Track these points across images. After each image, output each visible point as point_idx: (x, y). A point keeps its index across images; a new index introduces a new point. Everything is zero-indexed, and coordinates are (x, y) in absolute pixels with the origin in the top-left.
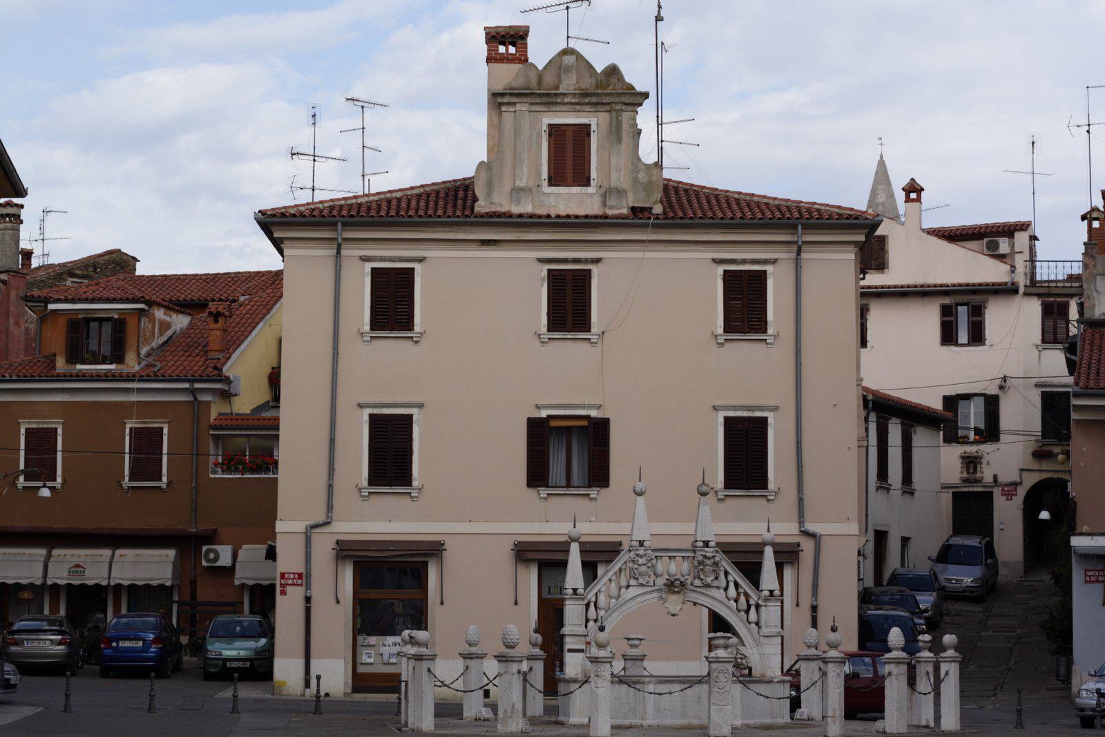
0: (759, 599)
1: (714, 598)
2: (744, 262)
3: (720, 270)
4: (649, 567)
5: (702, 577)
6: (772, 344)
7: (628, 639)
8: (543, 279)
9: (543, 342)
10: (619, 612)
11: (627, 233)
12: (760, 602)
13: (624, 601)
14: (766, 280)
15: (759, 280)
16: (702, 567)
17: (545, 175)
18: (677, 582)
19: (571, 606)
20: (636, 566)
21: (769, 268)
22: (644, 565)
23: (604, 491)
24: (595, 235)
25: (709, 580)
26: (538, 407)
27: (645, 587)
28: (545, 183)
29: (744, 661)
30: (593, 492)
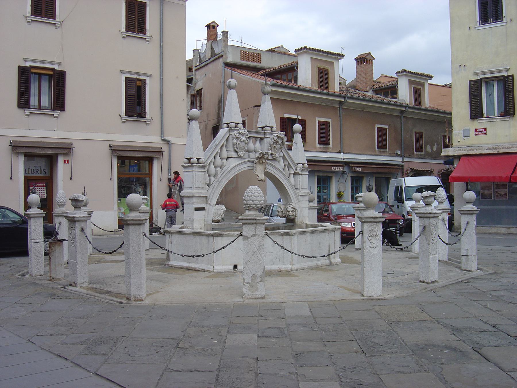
0: (296, 170)
4: (246, 143)
6: (148, 41)
9: (28, 22)
19: (196, 173)
20: (239, 142)
23: (62, 113)
26: (25, 60)
29: (294, 213)
30: (56, 113)
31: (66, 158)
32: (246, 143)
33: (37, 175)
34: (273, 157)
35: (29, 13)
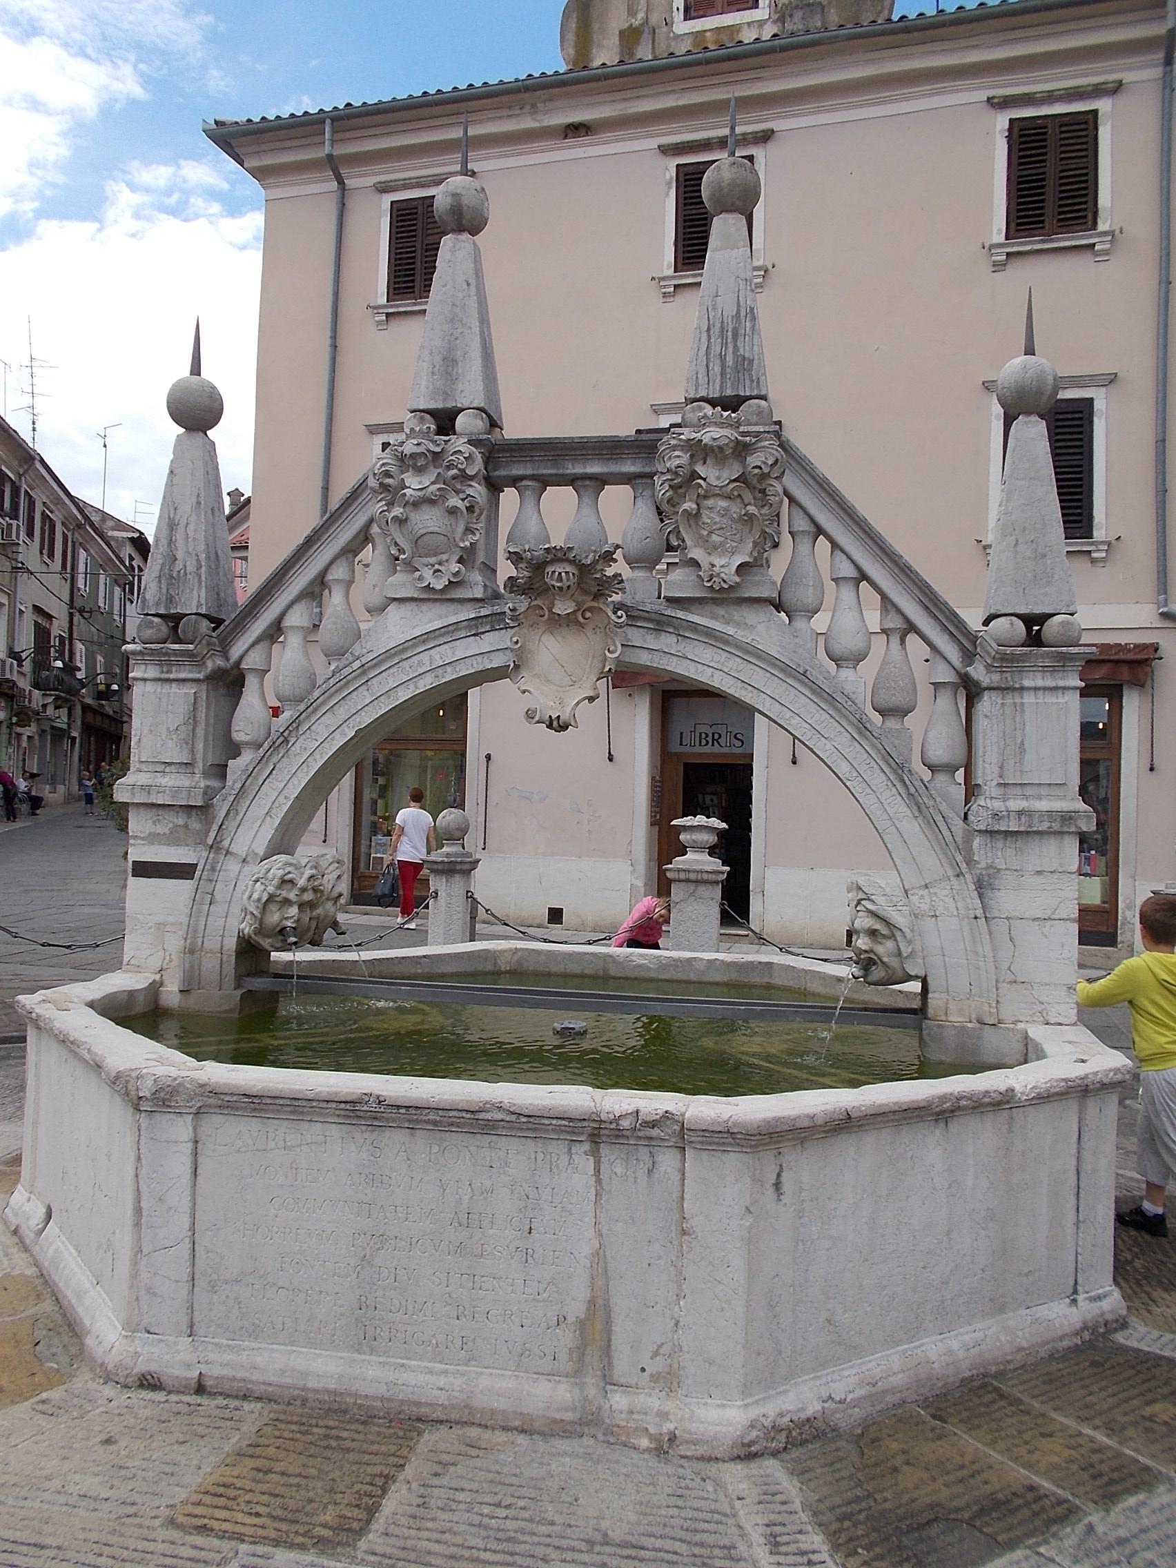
0: (969, 657)
1: (752, 653)
3: (1002, 121)
4: (453, 511)
8: (669, 183)
10: (342, 712)
11: (819, 70)
12: (978, 672)
13: (357, 664)
14: (1096, 129)
15: (1082, 130)
16: (689, 505)
18: (559, 568)
19: (150, 687)
20: (397, 511)
21: (1103, 105)
22: (431, 502)
24: (760, 84)
25: (726, 565)
26: (657, 410)
27: (452, 607)
28: (679, 16)
35: (669, 267)
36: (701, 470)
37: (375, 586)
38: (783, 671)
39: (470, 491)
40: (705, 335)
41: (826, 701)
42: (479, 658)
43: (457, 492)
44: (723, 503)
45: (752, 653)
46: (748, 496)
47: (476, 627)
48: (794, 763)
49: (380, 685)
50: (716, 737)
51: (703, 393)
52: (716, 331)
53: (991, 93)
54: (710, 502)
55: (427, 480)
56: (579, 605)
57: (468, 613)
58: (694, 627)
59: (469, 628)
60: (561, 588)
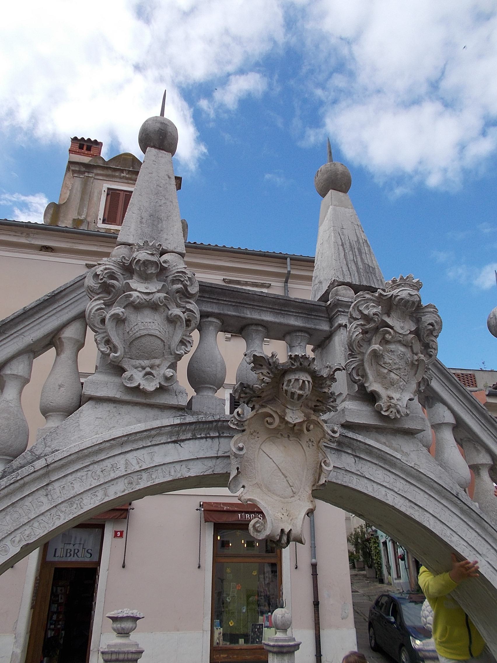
1: (414, 476)
2: (246, 284)
4: (172, 321)
5: (374, 386)
7: (115, 619)
13: (40, 464)
17: (101, 216)
18: (305, 377)
20: (117, 310)
22: (154, 307)
27: (152, 413)
31: (119, 528)
32: (172, 321)
33: (75, 559)
34: (378, 413)
36: (389, 321)
37: (60, 386)
38: (438, 493)
39: (188, 306)
40: (341, 247)
41: (474, 521)
42: (178, 466)
43: (178, 306)
44: (402, 349)
45: (414, 476)
46: (417, 347)
47: (176, 435)
48: (124, 567)
49: (61, 491)
50: (76, 551)
51: (348, 280)
52: (347, 246)
53: (225, 278)
54: (392, 347)
55: (154, 287)
56: (307, 415)
57: (169, 420)
58: (370, 450)
59: (171, 434)
60: (300, 396)
